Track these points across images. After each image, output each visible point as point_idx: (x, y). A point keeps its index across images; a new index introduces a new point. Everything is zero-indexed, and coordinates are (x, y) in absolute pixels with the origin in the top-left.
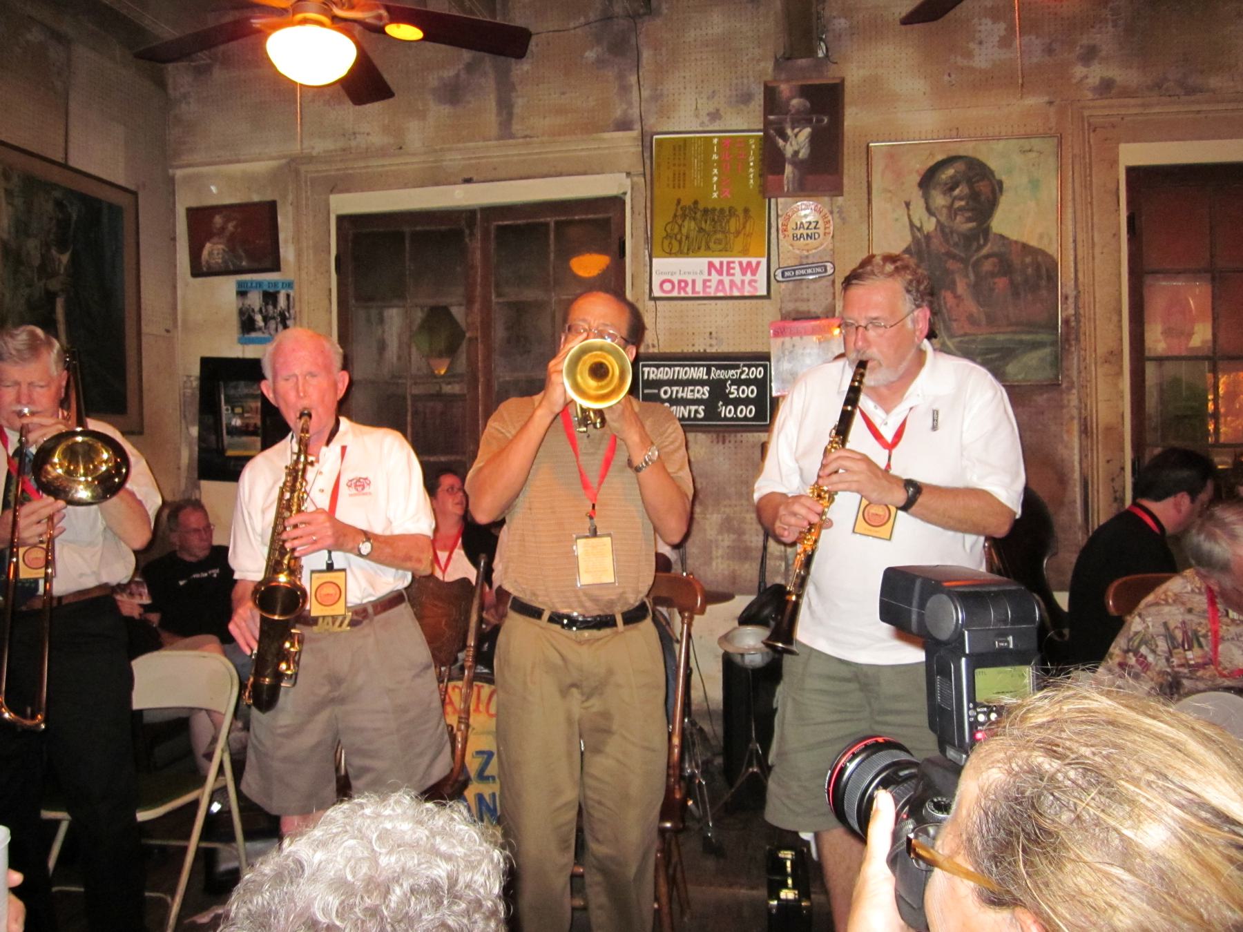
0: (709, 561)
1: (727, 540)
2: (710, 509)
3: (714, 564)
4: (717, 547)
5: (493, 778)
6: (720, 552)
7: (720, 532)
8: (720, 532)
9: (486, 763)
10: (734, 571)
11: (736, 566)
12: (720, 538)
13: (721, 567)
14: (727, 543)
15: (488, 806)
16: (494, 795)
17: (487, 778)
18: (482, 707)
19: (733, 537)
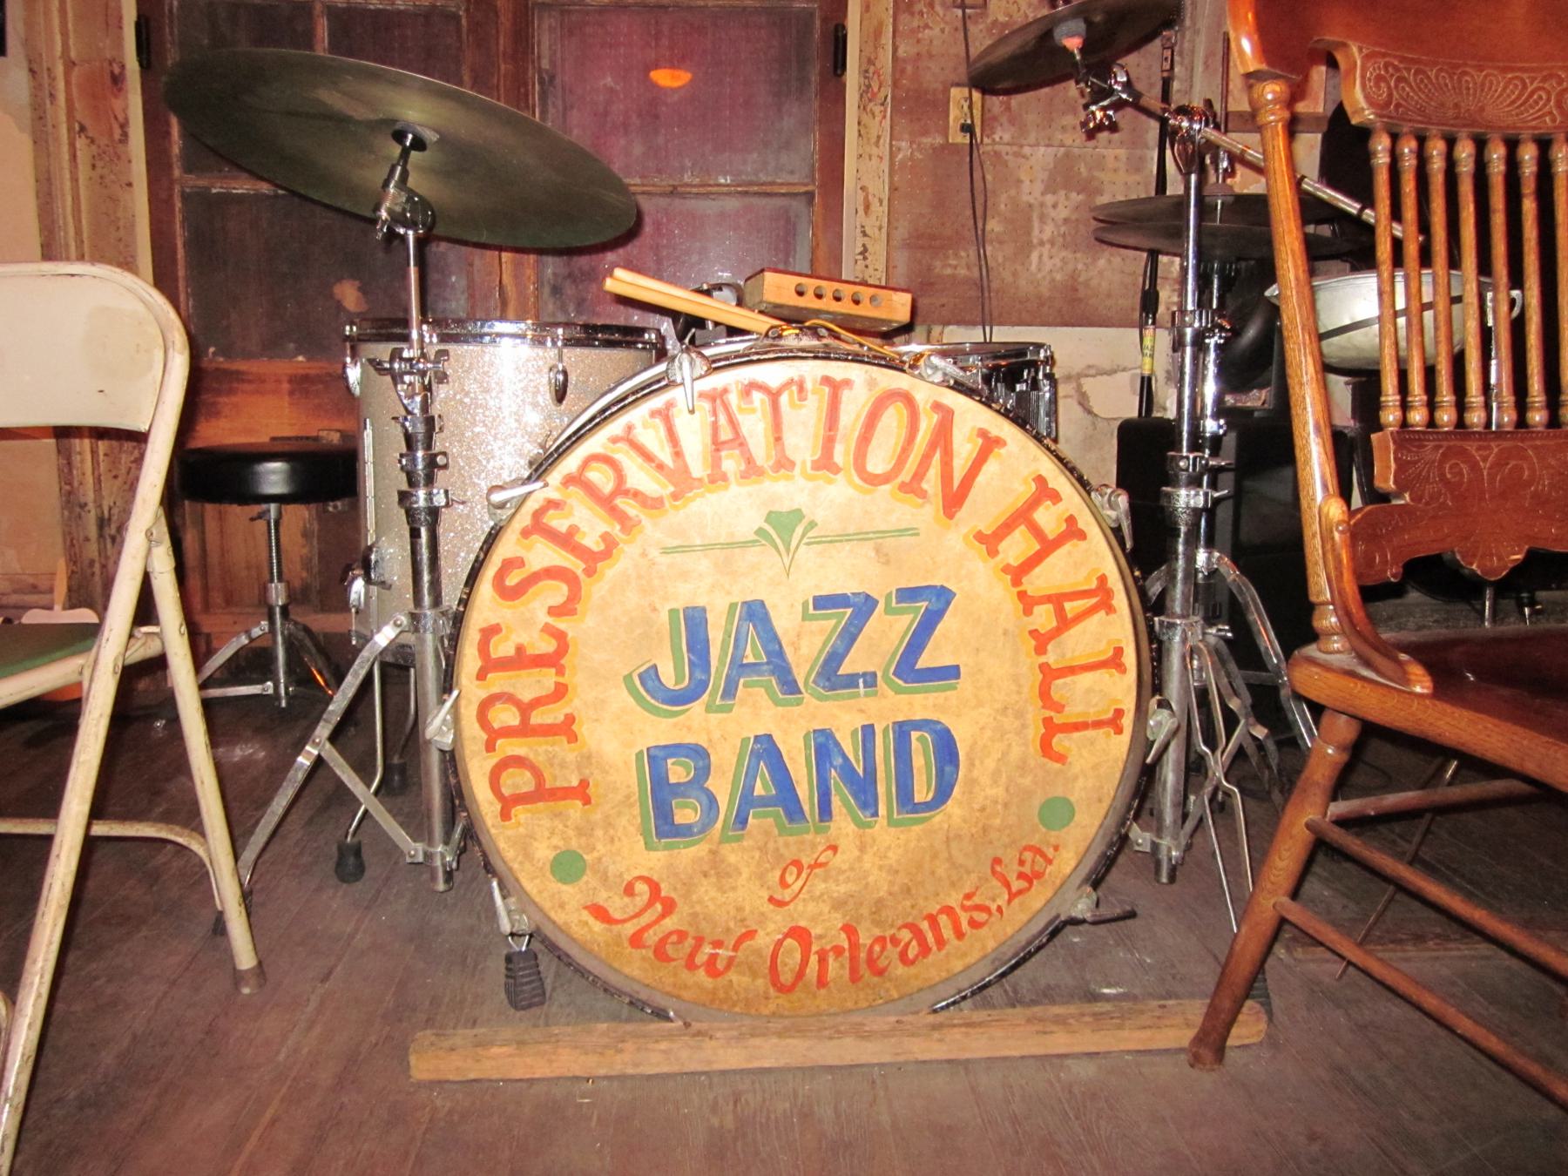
0: (1025, 248)
1: (1064, 206)
2: (1032, 138)
3: (1034, 256)
4: (1042, 218)
5: (870, 680)
6: (1049, 230)
7: (1050, 188)
8: (1050, 188)
9: (850, 636)
10: (1074, 276)
11: (1079, 262)
12: (1050, 199)
13: (1048, 265)
14: (1062, 213)
15: (847, 771)
16: (868, 731)
17: (851, 681)
18: (841, 454)
19: (1076, 198)
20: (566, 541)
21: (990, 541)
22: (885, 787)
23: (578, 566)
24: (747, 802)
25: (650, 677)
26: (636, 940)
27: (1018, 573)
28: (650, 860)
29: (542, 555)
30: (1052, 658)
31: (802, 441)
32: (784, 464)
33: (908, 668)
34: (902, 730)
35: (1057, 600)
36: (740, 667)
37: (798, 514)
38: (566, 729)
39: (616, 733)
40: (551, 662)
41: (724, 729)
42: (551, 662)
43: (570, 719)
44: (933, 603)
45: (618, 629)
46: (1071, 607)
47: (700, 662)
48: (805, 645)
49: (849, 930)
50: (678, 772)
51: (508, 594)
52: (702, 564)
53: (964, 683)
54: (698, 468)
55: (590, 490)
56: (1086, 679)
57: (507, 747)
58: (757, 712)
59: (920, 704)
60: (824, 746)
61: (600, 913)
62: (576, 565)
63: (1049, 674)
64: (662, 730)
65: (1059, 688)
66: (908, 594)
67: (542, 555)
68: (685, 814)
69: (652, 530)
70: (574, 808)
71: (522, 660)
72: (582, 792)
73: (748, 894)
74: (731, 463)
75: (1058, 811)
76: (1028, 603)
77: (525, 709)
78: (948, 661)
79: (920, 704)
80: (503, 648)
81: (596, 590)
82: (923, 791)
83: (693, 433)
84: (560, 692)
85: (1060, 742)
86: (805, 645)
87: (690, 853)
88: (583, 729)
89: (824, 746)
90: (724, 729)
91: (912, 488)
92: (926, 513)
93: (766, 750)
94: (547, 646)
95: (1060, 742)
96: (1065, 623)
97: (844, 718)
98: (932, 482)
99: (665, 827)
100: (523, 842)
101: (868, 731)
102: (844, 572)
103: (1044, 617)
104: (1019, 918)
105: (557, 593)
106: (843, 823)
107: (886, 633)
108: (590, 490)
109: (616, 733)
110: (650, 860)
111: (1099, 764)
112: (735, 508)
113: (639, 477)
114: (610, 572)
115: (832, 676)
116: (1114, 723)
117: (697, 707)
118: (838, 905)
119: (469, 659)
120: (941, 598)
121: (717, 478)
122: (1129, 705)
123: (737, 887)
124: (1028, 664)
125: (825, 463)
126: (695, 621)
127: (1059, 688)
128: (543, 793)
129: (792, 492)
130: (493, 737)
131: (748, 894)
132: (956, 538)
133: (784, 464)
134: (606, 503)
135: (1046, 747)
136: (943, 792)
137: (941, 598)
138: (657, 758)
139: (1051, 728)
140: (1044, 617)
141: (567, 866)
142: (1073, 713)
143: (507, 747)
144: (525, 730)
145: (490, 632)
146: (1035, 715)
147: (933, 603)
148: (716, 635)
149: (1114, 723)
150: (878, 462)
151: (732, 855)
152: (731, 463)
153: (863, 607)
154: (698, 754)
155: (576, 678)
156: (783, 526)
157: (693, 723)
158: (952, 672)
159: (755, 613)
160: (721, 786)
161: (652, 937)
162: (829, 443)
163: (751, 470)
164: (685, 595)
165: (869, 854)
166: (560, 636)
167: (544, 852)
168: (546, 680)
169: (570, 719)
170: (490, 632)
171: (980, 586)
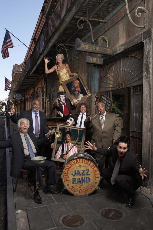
9: (84, 172)
16: (85, 178)
17: (84, 175)
18: (83, 162)
20: (68, 167)
21: (91, 167)
23: (69, 168)
24: (78, 182)
25: (73, 174)
26: (71, 190)
27: (93, 169)
28: (72, 185)
29: (67, 167)
30: (95, 174)
31: (81, 161)
32: (80, 163)
33: (87, 174)
34: (87, 178)
35: (95, 170)
36: (78, 174)
37: (81, 165)
38: (68, 177)
39: (71, 177)
40: (67, 173)
41: (77, 177)
42: (67, 173)
43: (68, 176)
45: (71, 171)
46: (96, 171)
47: (76, 173)
48: (81, 172)
49: (84, 190)
50: (74, 180)
51: (65, 169)
52: (76, 168)
53: (90, 175)
54: (76, 163)
55: (70, 164)
56: (97, 175)
57: (65, 178)
58: (78, 176)
59: (88, 176)
60: (82, 178)
61: (70, 188)
62: (69, 168)
63: (95, 175)
64: (73, 177)
65: (96, 175)
66: (87, 170)
67: (67, 167)
68: (74, 182)
70: (68, 182)
71: (66, 173)
72: (69, 181)
73: (78, 187)
74: (77, 162)
75: (96, 183)
76: (94, 170)
77: (66, 176)
78: (89, 174)
79: (88, 176)
80: (65, 172)
82: (88, 182)
84: (68, 175)
85: (96, 179)
86: (81, 172)
87: (74, 185)
88: (69, 177)
89: (82, 178)
90: (77, 177)
91: (87, 164)
92: (88, 165)
93: (79, 179)
94: (67, 172)
95: (96, 179)
96: (96, 172)
97: (83, 177)
98: (88, 164)
99: (73, 183)
100: (65, 184)
101: (85, 178)
102: (83, 169)
103: (95, 171)
104: (93, 190)
105: (68, 169)
106: (83, 183)
107: (86, 172)
108: (70, 164)
109: (71, 177)
110: (72, 185)
111: (98, 180)
112: (77, 165)
113: (72, 163)
114: (71, 168)
115: (83, 175)
116: (99, 177)
117: (75, 176)
118: (83, 188)
119: (63, 173)
120: (89, 170)
121: (77, 163)
122: (100, 176)
123: (77, 187)
124: (94, 174)
125: (82, 163)
126: (75, 171)
127: (96, 175)
128: (67, 181)
129: (80, 164)
130: (64, 177)
131: (78, 187)
132: (90, 167)
133: (80, 163)
134: (71, 165)
135: (95, 179)
136: (89, 182)
137: (89, 170)
138: (73, 179)
139: (95, 178)
140: (95, 171)
141: (68, 185)
142: (97, 177)
143: (65, 178)
144: (66, 177)
145: (64, 172)
146: (94, 177)
149: (99, 177)
150: (85, 163)
151: (77, 185)
152: (77, 162)
153: (84, 170)
154: (75, 179)
155: (69, 174)
156: (80, 166)
157: (75, 177)
158: (90, 174)
159: (78, 171)
160: (77, 181)
161: (73, 189)
162: (82, 162)
163: (78, 163)
164: (75, 170)
165: (84, 185)
166: (68, 172)
167: (67, 184)
168: (67, 174)
169: (68, 176)
170: (64, 172)
171: (91, 169)
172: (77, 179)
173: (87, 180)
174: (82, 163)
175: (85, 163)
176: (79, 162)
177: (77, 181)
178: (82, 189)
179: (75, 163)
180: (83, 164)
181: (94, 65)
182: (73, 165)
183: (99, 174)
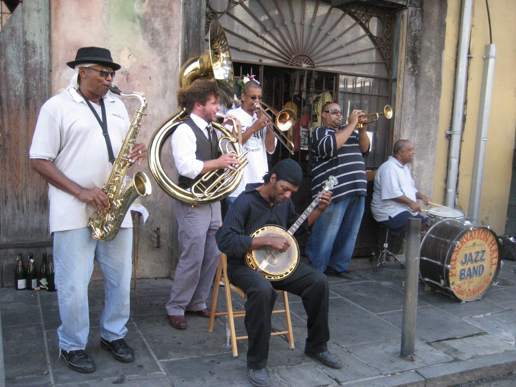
9: (478, 255)
22: (478, 272)
25: (462, 261)
27: (490, 248)
31: (476, 236)
39: (459, 267)
44: (484, 251)
50: (463, 272)
59: (482, 263)
64: (462, 267)
66: (482, 251)
68: (463, 277)
69: (465, 245)
76: (491, 251)
79: (482, 263)
81: (460, 252)
83: (469, 236)
84: (455, 264)
89: (474, 268)
90: (466, 267)
91: (484, 240)
102: (477, 249)
114: (461, 250)
126: (466, 254)
132: (486, 245)
133: (475, 238)
137: (484, 251)
140: (492, 253)
147: (484, 251)
148: (468, 256)
151: (466, 281)
153: (479, 252)
156: (474, 244)
160: (466, 274)
165: (476, 280)
166: (456, 257)
172: (466, 270)
173: (480, 271)
174: (478, 238)
175: (482, 237)
176: (473, 236)
177: (466, 274)
178: (472, 289)
179: (467, 240)
180: (479, 240)
181: (416, 70)
182: (465, 243)
183: (496, 257)
